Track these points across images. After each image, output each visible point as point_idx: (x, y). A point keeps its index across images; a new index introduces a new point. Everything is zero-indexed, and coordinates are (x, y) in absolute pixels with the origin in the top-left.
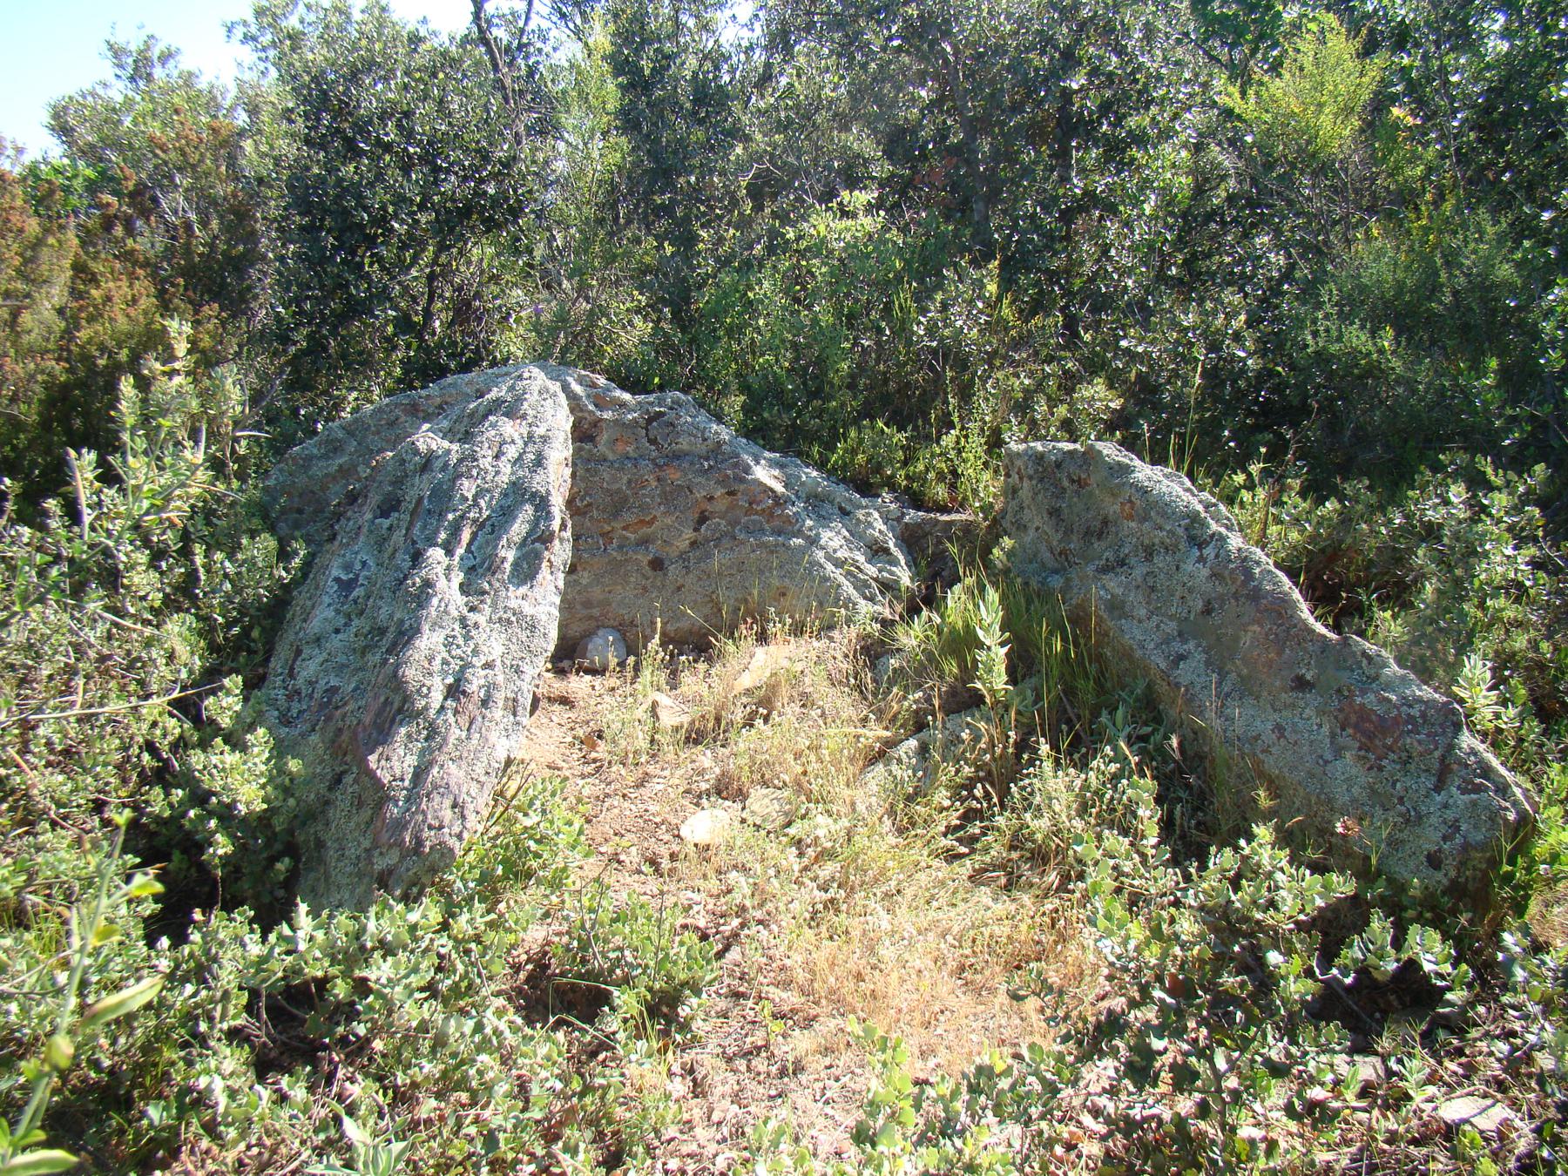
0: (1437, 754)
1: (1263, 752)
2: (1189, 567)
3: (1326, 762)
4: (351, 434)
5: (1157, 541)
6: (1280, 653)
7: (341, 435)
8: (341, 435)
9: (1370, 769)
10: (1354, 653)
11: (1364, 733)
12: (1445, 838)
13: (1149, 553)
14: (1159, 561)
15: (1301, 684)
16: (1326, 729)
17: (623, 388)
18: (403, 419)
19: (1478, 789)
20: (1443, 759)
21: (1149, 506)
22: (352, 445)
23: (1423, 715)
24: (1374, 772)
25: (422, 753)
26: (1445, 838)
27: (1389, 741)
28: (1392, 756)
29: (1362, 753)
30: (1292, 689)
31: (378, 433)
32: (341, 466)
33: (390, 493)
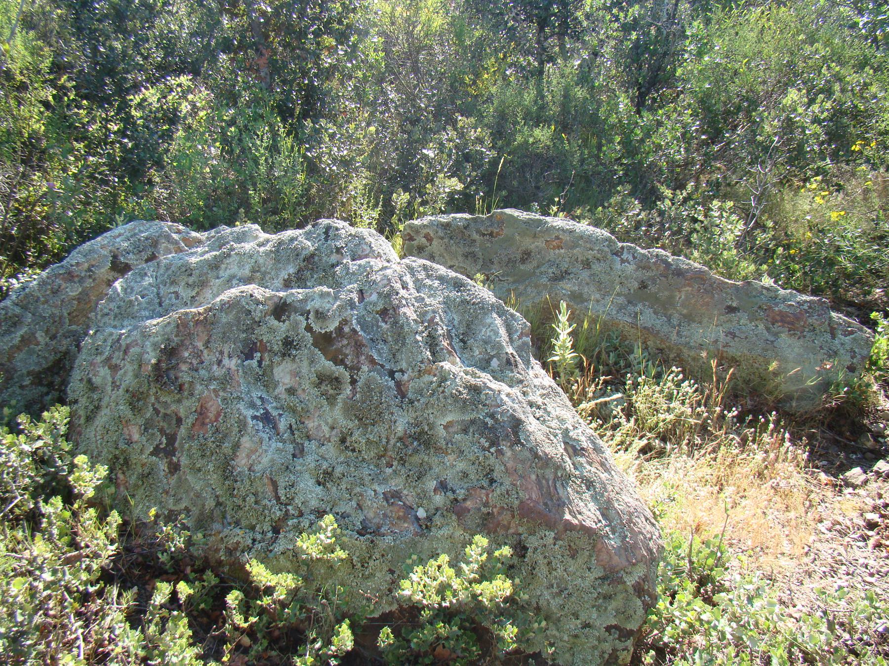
0: (827, 323)
1: (724, 347)
2: (618, 266)
3: (772, 342)
4: (25, 308)
5: (590, 257)
6: (713, 297)
7: (18, 310)
8: (18, 310)
9: (799, 338)
10: (756, 289)
11: (789, 323)
12: (852, 358)
13: (587, 264)
14: (597, 267)
15: (731, 310)
16: (761, 326)
17: (198, 230)
18: (64, 285)
19: (852, 333)
20: (829, 324)
21: (558, 238)
22: (29, 318)
23: (810, 307)
24: (802, 340)
25: (594, 498)
26: (852, 358)
27: (802, 323)
28: (807, 330)
29: (792, 332)
30: (727, 313)
31: (47, 302)
32: (22, 337)
33: (245, 340)
